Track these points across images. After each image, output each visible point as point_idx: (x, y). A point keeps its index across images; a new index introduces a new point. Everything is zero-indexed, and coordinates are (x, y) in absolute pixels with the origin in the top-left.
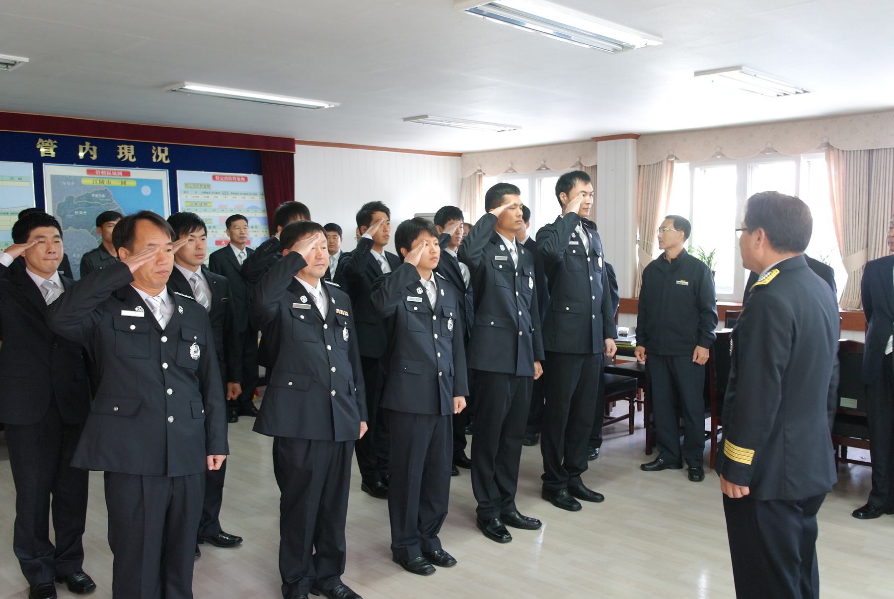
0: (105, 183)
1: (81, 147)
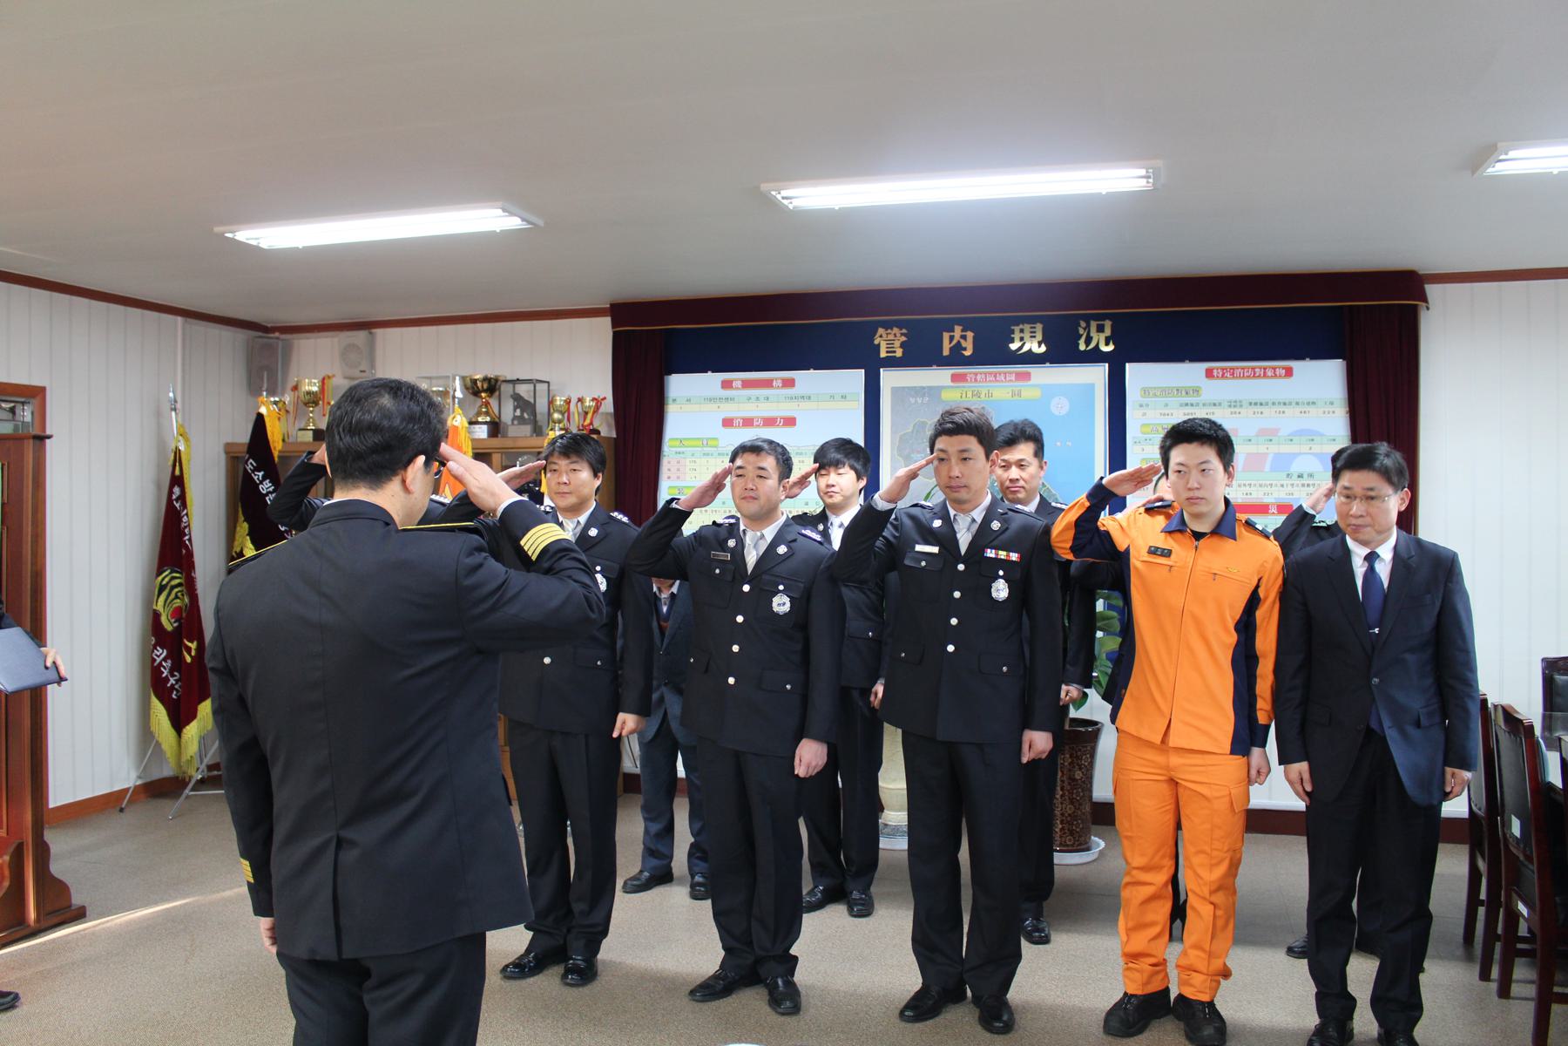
0: (983, 396)
1: (946, 336)
